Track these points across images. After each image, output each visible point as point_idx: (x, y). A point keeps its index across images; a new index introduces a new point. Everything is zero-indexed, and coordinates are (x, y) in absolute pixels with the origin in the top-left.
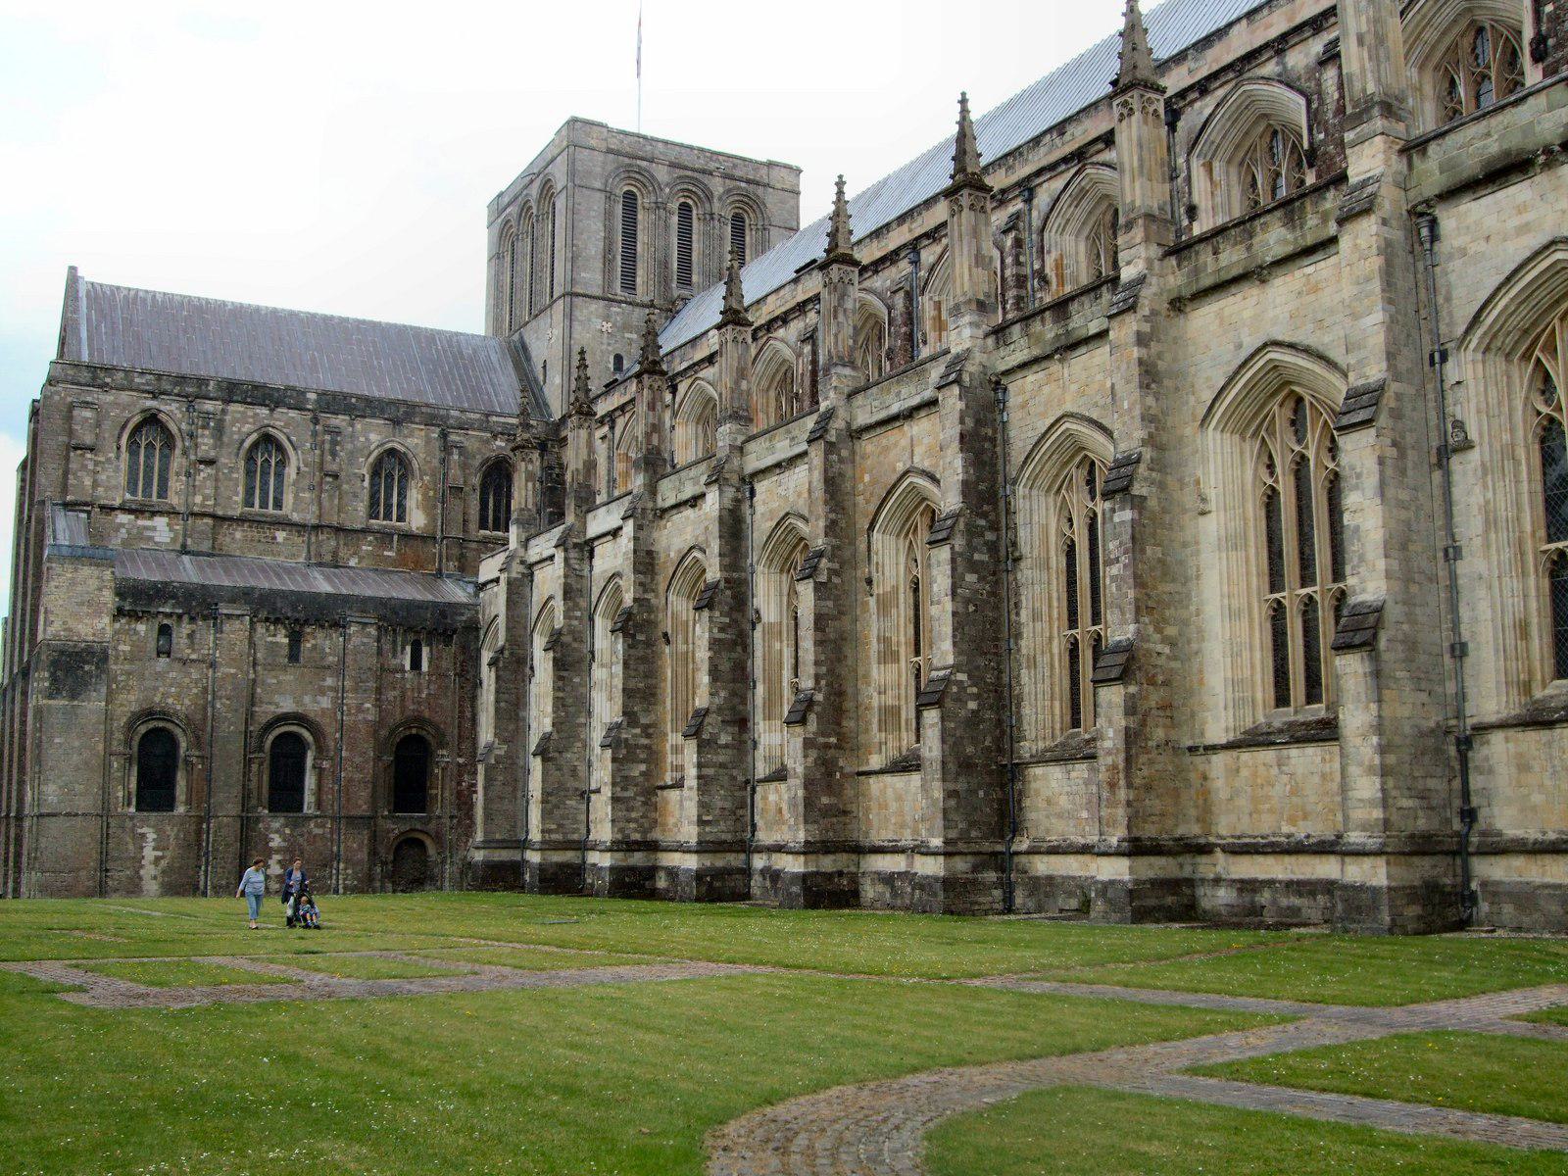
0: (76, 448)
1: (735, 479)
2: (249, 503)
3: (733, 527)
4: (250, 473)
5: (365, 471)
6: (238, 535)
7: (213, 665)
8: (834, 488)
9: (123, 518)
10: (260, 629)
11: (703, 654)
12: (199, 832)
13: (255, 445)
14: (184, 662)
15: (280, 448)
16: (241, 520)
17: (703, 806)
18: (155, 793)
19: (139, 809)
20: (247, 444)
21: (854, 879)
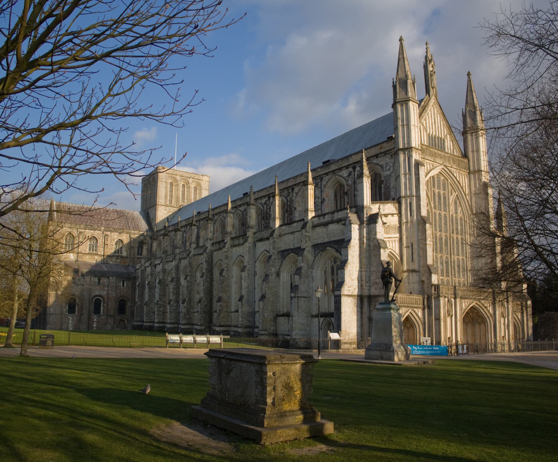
1: (178, 259)
2: (90, 250)
3: (177, 267)
5: (114, 244)
6: (87, 257)
7: (83, 285)
8: (190, 264)
10: (92, 278)
11: (171, 290)
12: (80, 318)
14: (78, 285)
15: (96, 239)
16: (88, 254)
17: (171, 316)
21: (192, 329)
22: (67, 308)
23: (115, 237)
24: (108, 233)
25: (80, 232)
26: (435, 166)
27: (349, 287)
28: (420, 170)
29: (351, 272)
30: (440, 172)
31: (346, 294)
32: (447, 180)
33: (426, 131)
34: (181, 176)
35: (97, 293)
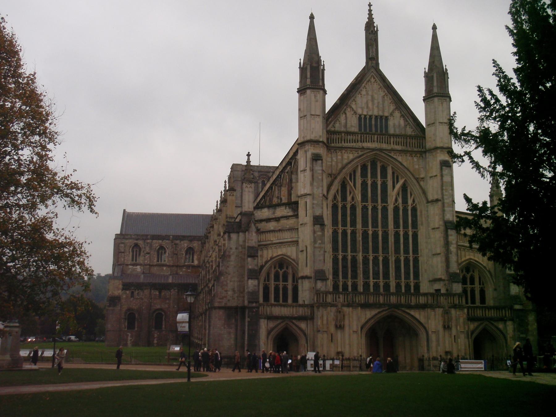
0: (120, 252)
4: (158, 255)
6: (155, 269)
9: (130, 267)
10: (152, 291)
13: (159, 249)
14: (137, 299)
15: (165, 249)
18: (131, 326)
19: (128, 329)
20: (157, 248)
22: (126, 324)
23: (186, 245)
24: (178, 242)
25: (148, 243)
26: (360, 153)
27: (221, 299)
28: (314, 165)
29: (225, 283)
30: (375, 158)
31: (215, 305)
33: (355, 113)
34: (259, 172)
35: (158, 307)
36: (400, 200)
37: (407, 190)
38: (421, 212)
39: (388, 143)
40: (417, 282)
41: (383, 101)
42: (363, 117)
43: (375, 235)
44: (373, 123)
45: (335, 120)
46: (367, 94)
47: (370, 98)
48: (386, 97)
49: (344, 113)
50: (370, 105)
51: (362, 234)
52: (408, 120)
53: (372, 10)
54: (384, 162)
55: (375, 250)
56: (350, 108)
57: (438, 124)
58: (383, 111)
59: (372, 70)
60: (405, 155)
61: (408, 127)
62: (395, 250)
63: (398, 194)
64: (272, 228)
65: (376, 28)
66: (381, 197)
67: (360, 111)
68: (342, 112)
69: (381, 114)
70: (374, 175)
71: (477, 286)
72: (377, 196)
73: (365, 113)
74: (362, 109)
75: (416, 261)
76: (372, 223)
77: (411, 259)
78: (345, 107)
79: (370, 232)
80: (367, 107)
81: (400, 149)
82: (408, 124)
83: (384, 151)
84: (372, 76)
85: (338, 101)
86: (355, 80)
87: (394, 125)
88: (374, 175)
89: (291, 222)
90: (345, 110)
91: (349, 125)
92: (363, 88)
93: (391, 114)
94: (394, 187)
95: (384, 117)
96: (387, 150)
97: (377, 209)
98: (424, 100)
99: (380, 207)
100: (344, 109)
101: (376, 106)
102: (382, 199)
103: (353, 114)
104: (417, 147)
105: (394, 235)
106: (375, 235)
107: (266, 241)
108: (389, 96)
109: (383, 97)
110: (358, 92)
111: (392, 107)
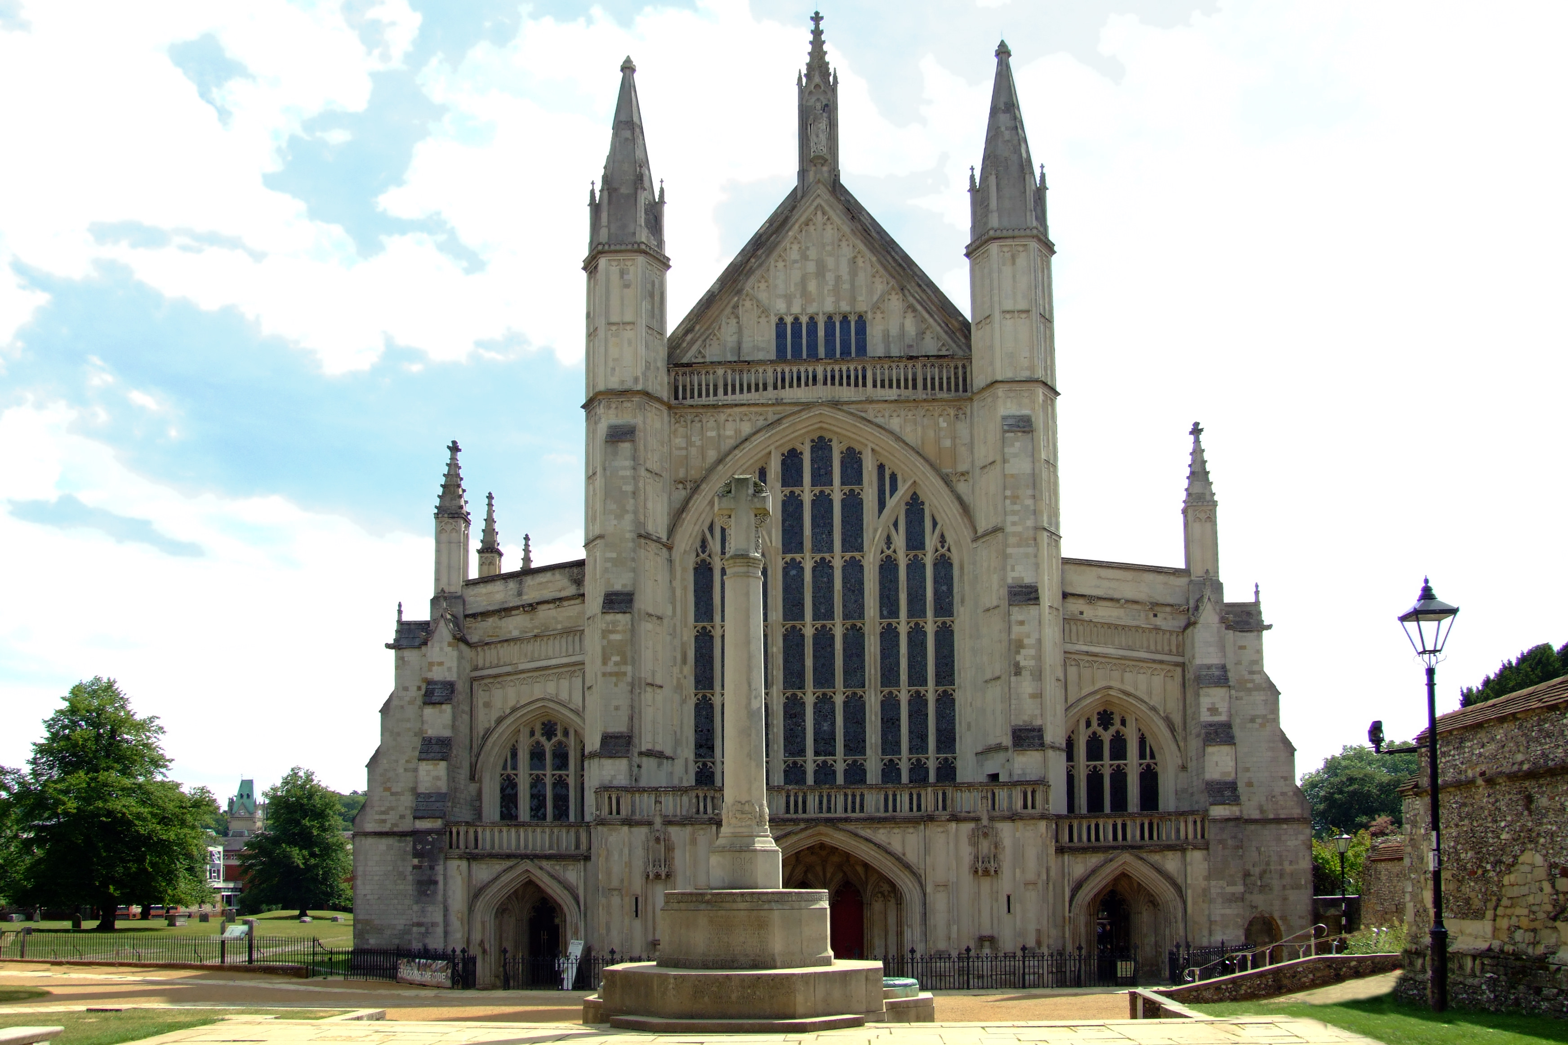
30: (821, 428)
32: (866, 445)
36: (900, 541)
37: (923, 509)
38: (962, 568)
39: (856, 385)
40: (946, 759)
41: (853, 273)
42: (789, 320)
43: (824, 639)
44: (821, 333)
45: (708, 332)
46: (805, 257)
47: (811, 267)
48: (860, 261)
49: (732, 317)
50: (812, 286)
51: (785, 637)
52: (926, 316)
53: (822, 32)
54: (849, 438)
55: (824, 677)
56: (751, 300)
57: (997, 316)
58: (853, 300)
59: (819, 191)
60: (910, 414)
61: (928, 336)
62: (882, 675)
63: (896, 525)
64: (515, 633)
65: (831, 79)
66: (843, 534)
67: (780, 306)
68: (728, 310)
69: (845, 307)
70: (822, 476)
71: (1133, 765)
72: (830, 533)
73: (796, 309)
74: (788, 299)
75: (946, 702)
76: (814, 605)
77: (931, 698)
78: (736, 299)
79: (809, 632)
80: (805, 293)
81: (893, 398)
82: (927, 328)
83: (845, 407)
84: (816, 208)
85: (717, 286)
86: (767, 225)
87: (886, 336)
88: (822, 476)
89: (570, 611)
90: (736, 307)
91: (746, 346)
92: (792, 243)
93: (876, 307)
94: (882, 505)
95: (853, 319)
96: (853, 402)
97: (832, 568)
98: (967, 255)
99: (838, 563)
100: (731, 304)
101: (831, 288)
102: (844, 541)
103: (760, 317)
104: (949, 389)
105: (882, 634)
106: (824, 639)
107: (498, 666)
108: (868, 254)
109: (854, 261)
110: (775, 255)
111: (880, 287)
